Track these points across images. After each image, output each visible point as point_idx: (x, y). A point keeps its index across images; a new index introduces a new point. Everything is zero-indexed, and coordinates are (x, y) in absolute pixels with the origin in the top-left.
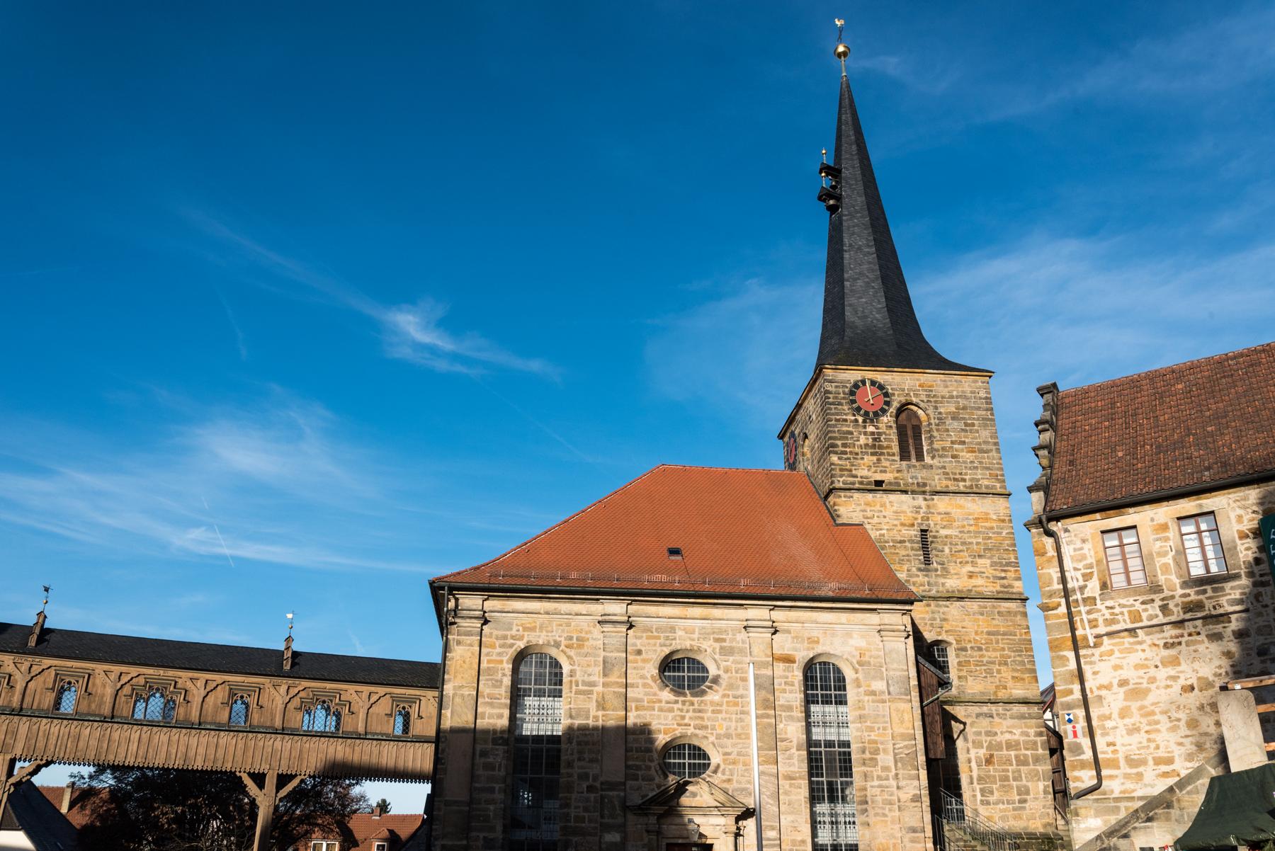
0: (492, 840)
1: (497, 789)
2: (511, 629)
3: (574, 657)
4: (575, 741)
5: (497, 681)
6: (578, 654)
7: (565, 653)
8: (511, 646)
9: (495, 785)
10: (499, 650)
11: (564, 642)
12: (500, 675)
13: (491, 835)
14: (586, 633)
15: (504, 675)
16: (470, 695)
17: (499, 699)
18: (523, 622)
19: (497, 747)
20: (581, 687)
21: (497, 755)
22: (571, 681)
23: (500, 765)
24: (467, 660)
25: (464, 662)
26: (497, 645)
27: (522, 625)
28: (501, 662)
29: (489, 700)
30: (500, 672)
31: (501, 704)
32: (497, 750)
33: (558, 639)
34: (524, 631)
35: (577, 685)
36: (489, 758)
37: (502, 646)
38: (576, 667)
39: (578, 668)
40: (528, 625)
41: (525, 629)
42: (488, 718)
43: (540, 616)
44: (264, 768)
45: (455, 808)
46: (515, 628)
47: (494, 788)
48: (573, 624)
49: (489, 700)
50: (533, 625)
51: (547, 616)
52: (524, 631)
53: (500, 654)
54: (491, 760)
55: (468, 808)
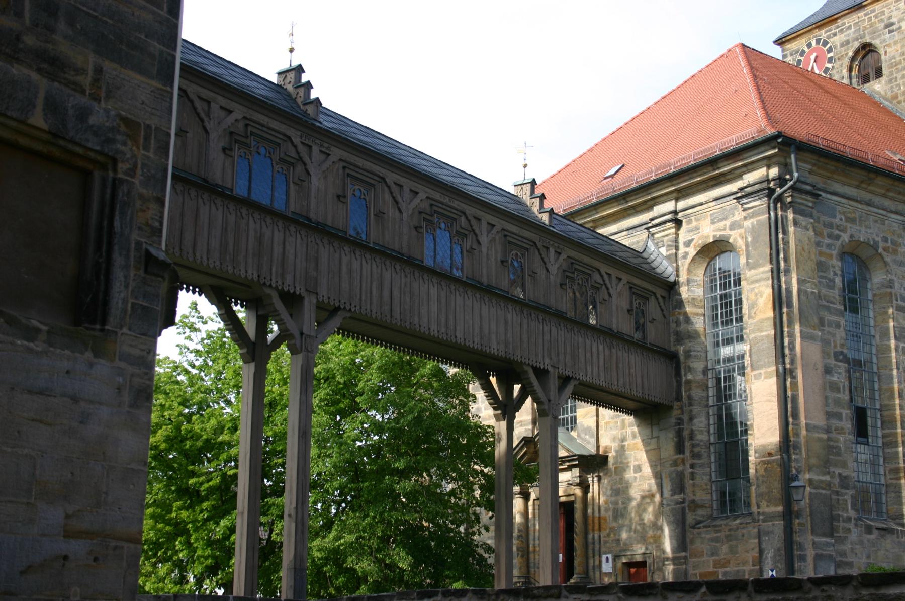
0: (846, 477)
1: (844, 415)
2: (835, 217)
3: (891, 264)
4: (901, 368)
5: (830, 280)
6: (894, 261)
7: (883, 258)
8: (838, 238)
9: (842, 411)
10: (827, 241)
11: (881, 245)
12: (832, 273)
13: (845, 473)
14: (898, 237)
15: (835, 274)
16: (812, 293)
17: (834, 303)
18: (845, 210)
19: (840, 364)
20: (900, 303)
21: (840, 373)
22: (891, 293)
23: (844, 386)
24: (806, 247)
25: (803, 249)
26: (825, 234)
27: (844, 213)
28: (831, 256)
29: (826, 304)
30: (831, 269)
31: (836, 310)
32: (839, 367)
33: (877, 239)
34: (846, 221)
35: (897, 300)
36: (833, 376)
37: (830, 236)
38: (893, 277)
39: (895, 279)
40: (849, 215)
41: (848, 220)
42: (828, 326)
43: (860, 206)
44: (545, 363)
45: (816, 435)
46: (838, 216)
47: (841, 414)
48: (887, 222)
49: (826, 304)
50: (853, 215)
51: (865, 207)
52: (846, 221)
53: (829, 246)
54: (835, 379)
55: (825, 436)
